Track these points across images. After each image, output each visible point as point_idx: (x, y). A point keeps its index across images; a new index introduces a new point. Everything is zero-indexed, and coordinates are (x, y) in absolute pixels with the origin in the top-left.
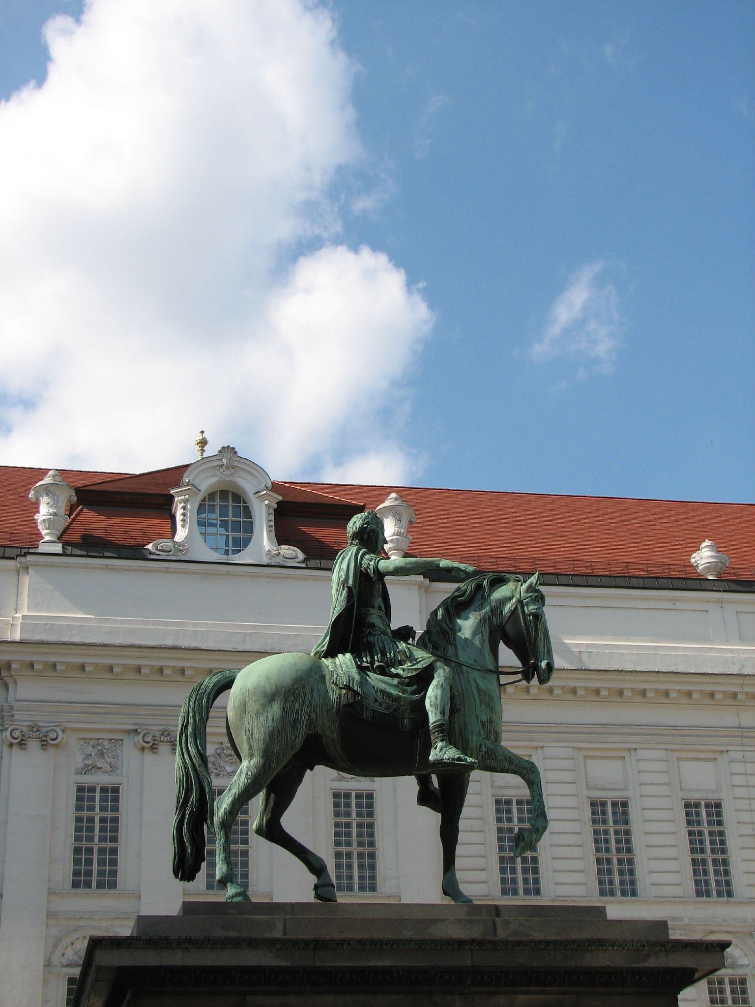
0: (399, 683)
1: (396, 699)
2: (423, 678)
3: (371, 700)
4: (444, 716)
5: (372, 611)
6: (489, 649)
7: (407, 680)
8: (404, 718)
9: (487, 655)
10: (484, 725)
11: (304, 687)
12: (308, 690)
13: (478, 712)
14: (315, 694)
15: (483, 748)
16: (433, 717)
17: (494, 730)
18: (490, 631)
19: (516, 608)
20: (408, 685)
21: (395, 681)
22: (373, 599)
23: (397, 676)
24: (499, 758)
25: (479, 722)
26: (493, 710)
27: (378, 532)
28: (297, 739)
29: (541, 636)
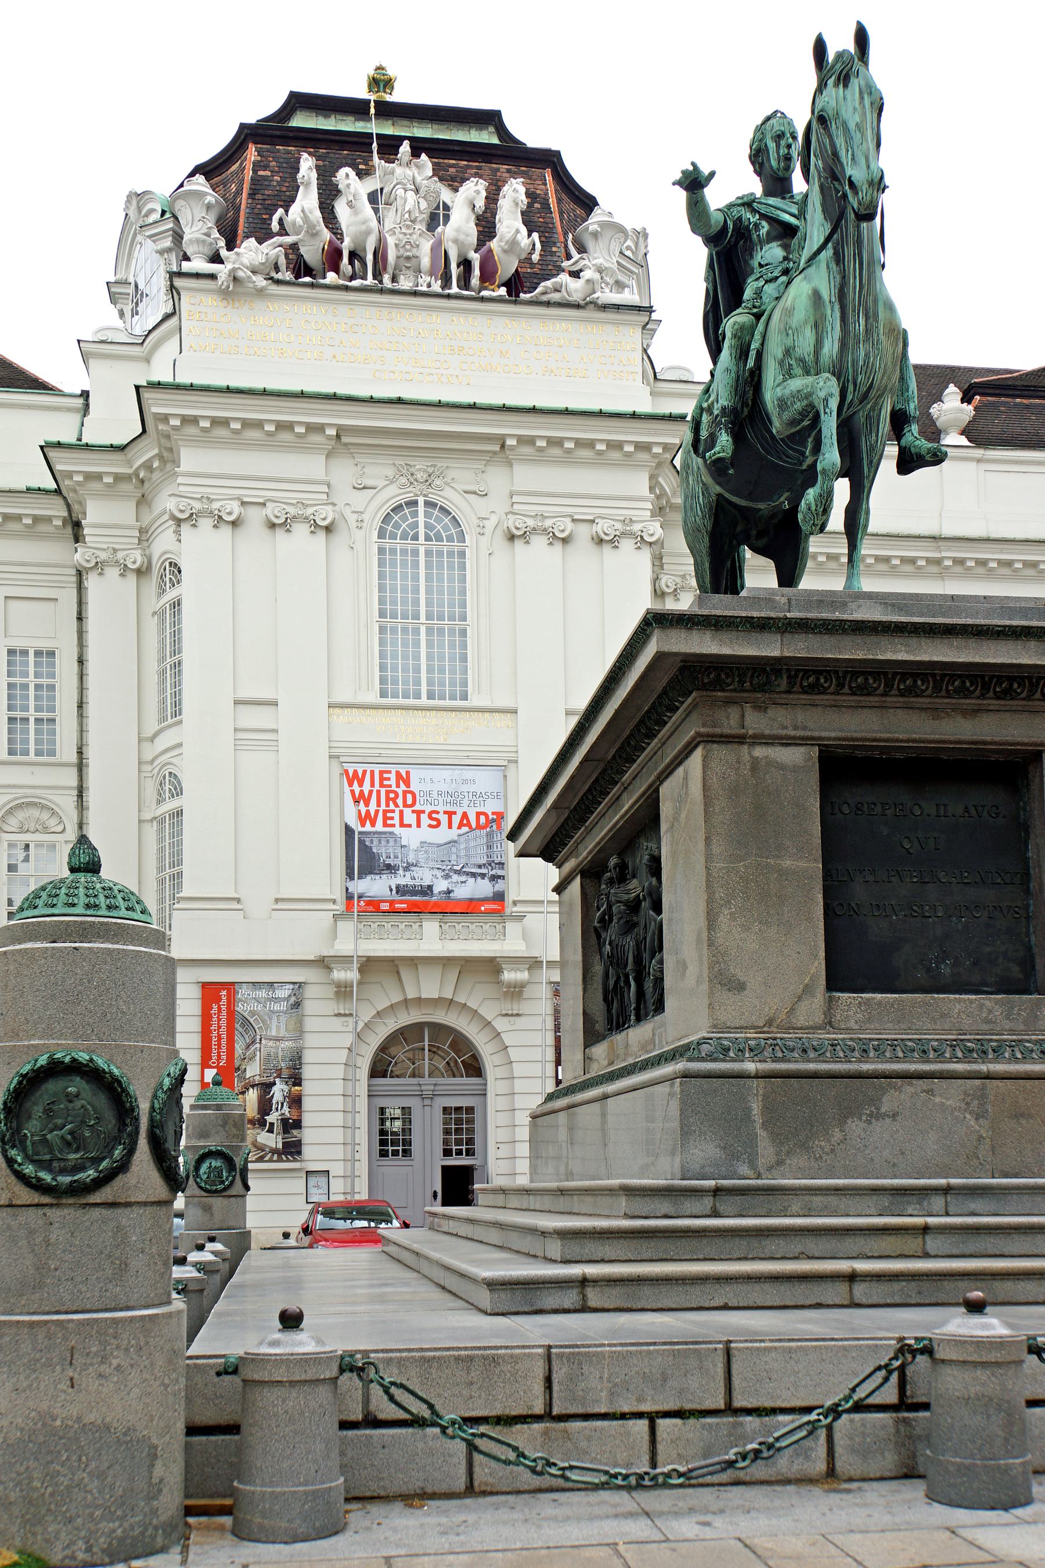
10: (781, 363)
22: (751, 262)
26: (790, 332)
27: (766, 145)
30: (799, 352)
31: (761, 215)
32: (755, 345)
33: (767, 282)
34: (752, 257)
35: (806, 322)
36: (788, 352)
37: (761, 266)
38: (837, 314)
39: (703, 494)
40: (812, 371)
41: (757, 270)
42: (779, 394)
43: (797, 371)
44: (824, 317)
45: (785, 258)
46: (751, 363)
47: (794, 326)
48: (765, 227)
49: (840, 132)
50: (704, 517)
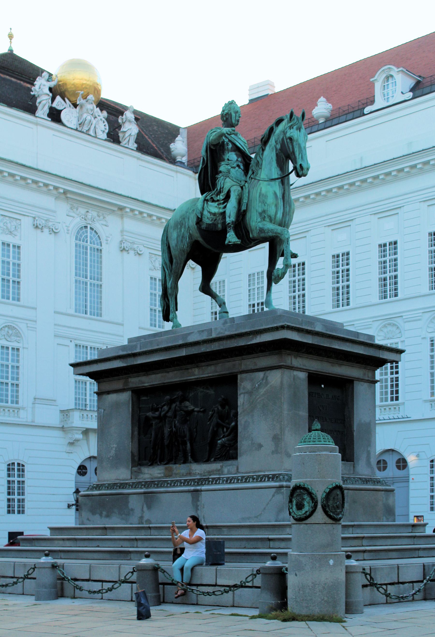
0: (218, 205)
1: (214, 214)
2: (227, 197)
3: (206, 217)
4: (230, 218)
5: (223, 163)
6: (276, 165)
7: (222, 201)
8: (218, 224)
9: (273, 170)
10: (260, 214)
11: (184, 219)
12: (186, 220)
13: (257, 208)
14: (190, 221)
15: (258, 228)
16: (228, 220)
17: (267, 215)
18: (277, 155)
19: (283, 137)
20: (223, 203)
21: (217, 203)
23: (218, 201)
24: (266, 231)
25: (258, 214)
28: (184, 247)
29: (296, 150)
30: (269, 213)
31: (229, 139)
32: (245, 201)
33: (232, 167)
34: (224, 154)
35: (273, 203)
36: (264, 211)
37: (228, 160)
38: (282, 203)
39: (189, 238)
40: (273, 222)
41: (226, 160)
42: (261, 226)
43: (268, 219)
44: (278, 203)
45: (237, 160)
46: (244, 208)
47: (268, 202)
48: (230, 146)
49: (297, 146)
50: (188, 247)
